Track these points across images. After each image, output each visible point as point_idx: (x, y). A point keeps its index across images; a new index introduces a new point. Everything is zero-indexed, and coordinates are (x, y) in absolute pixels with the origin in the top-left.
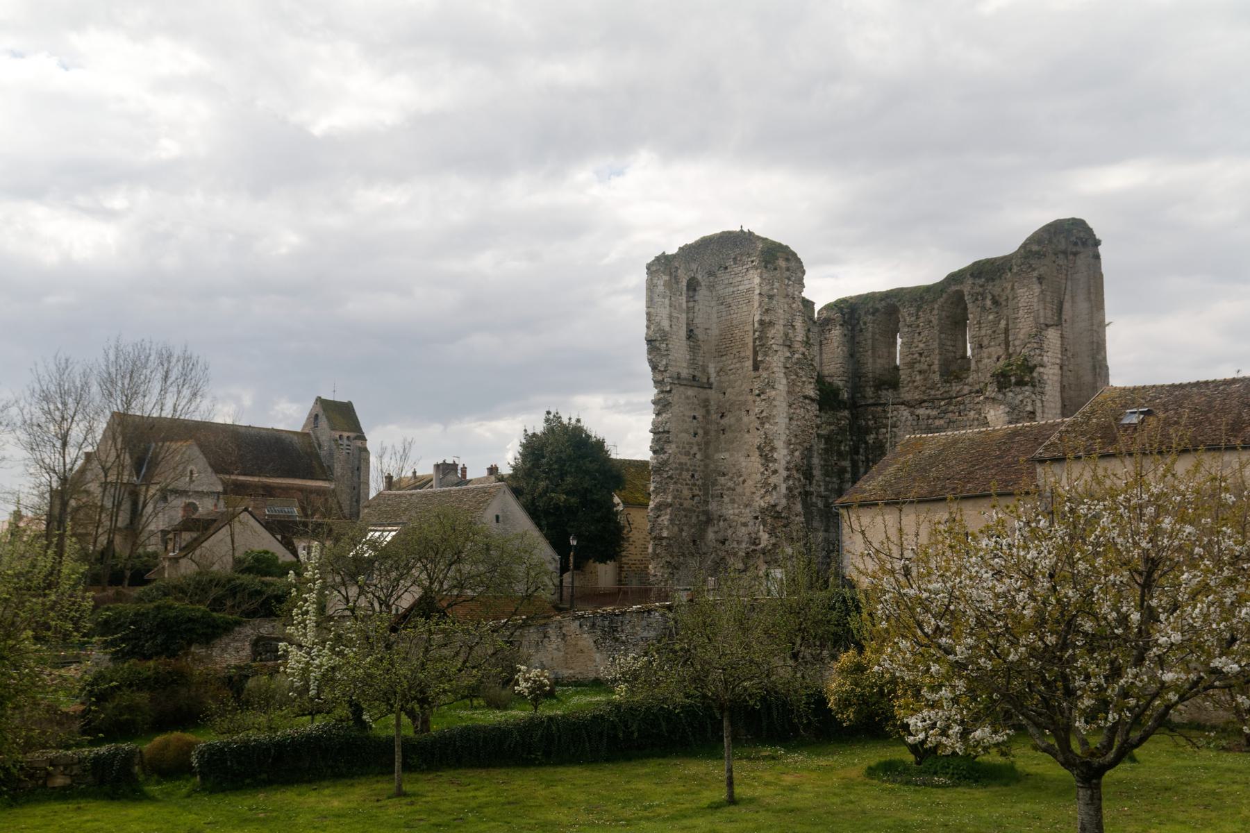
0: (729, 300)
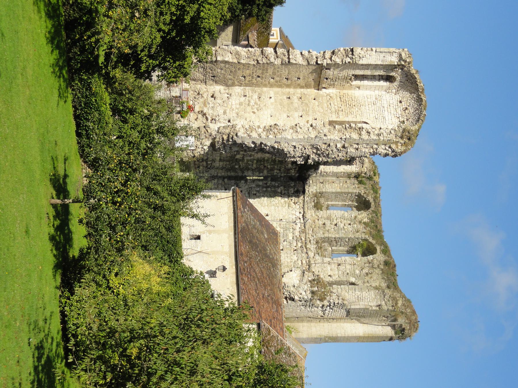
0: (378, 104)
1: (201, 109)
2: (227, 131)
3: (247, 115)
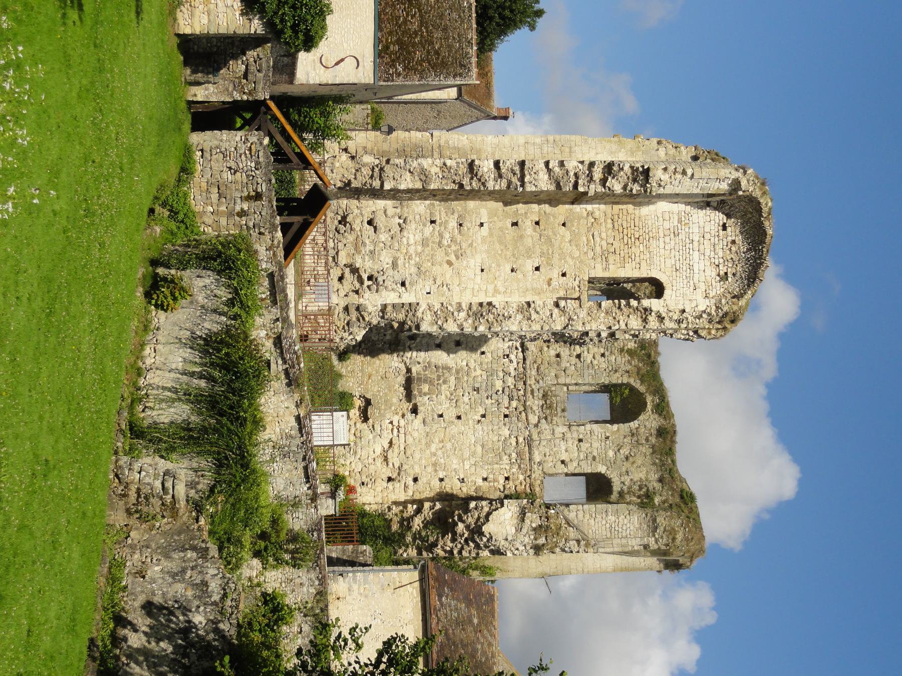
1: (349, 261)
2: (401, 317)
3: (437, 270)
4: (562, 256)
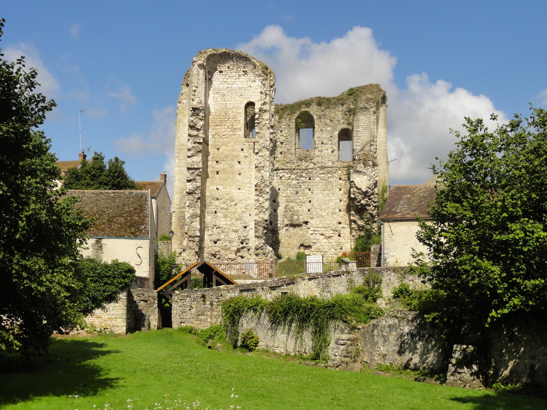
1: (234, 253)
2: (261, 229)
3: (239, 211)
4: (234, 150)
